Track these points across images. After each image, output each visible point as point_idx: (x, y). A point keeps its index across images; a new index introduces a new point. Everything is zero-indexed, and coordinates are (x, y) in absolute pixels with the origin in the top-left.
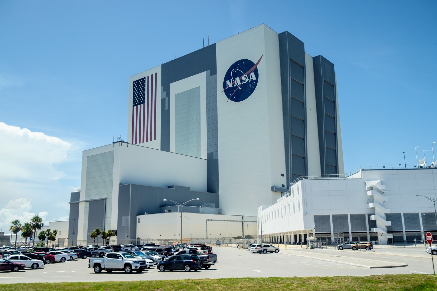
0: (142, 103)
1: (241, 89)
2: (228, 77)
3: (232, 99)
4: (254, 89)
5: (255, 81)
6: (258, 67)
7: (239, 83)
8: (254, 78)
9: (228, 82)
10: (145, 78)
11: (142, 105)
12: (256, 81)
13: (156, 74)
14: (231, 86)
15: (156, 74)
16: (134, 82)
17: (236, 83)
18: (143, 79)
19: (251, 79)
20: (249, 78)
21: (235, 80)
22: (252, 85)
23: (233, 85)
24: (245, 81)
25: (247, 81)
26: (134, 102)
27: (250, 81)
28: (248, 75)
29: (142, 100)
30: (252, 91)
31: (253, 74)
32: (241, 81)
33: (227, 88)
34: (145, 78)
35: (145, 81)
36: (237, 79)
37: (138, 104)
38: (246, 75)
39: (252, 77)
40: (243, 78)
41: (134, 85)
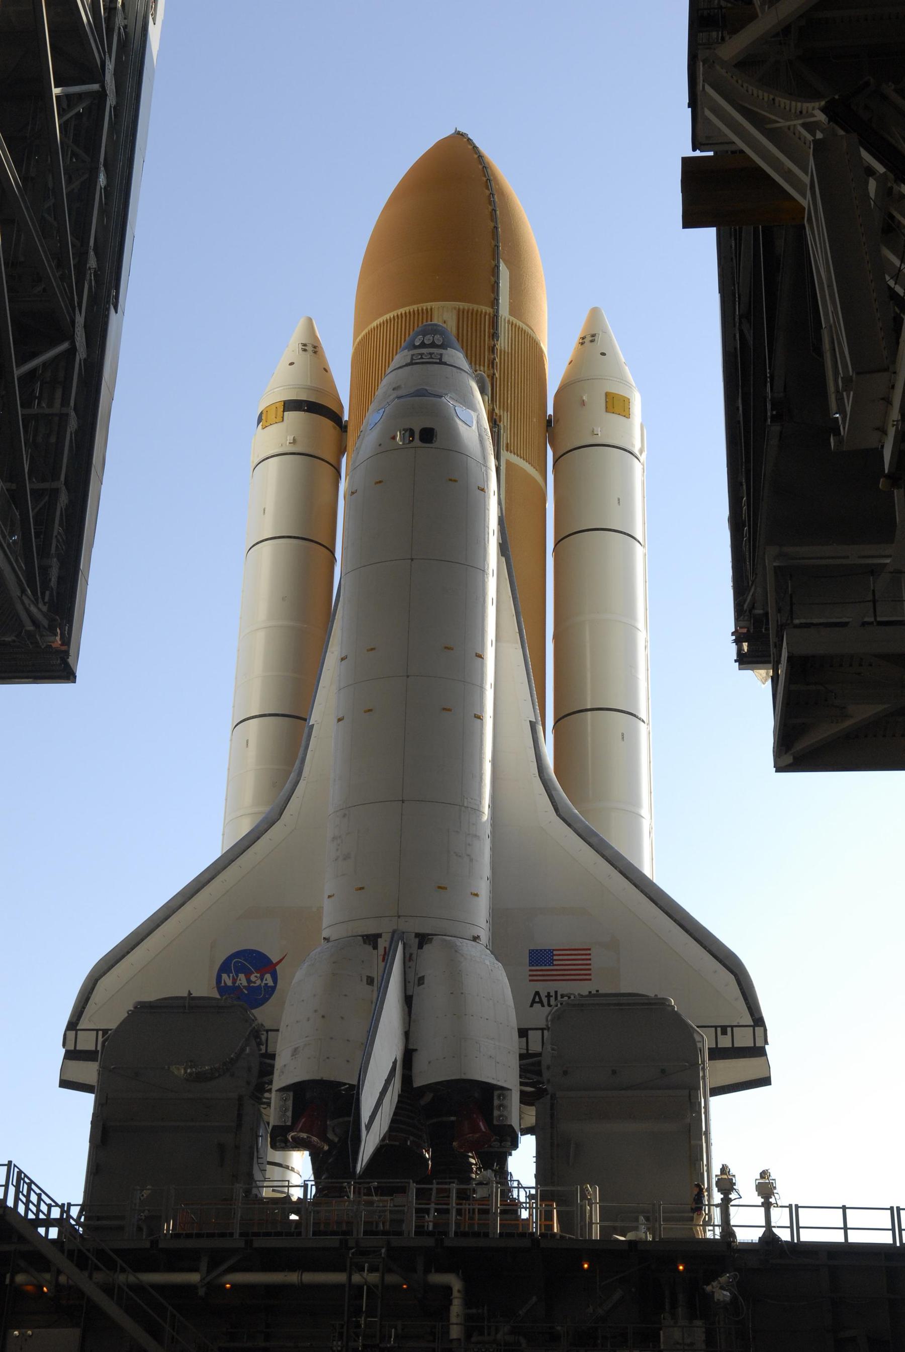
2: (225, 967)
4: (268, 999)
5: (270, 987)
6: (277, 968)
7: (245, 983)
8: (271, 983)
9: (224, 976)
12: (273, 989)
14: (229, 983)
17: (238, 982)
19: (264, 982)
20: (262, 980)
24: (255, 983)
25: (258, 982)
30: (265, 1000)
31: (268, 976)
32: (249, 981)
33: (223, 984)
36: (242, 976)
40: (253, 978)
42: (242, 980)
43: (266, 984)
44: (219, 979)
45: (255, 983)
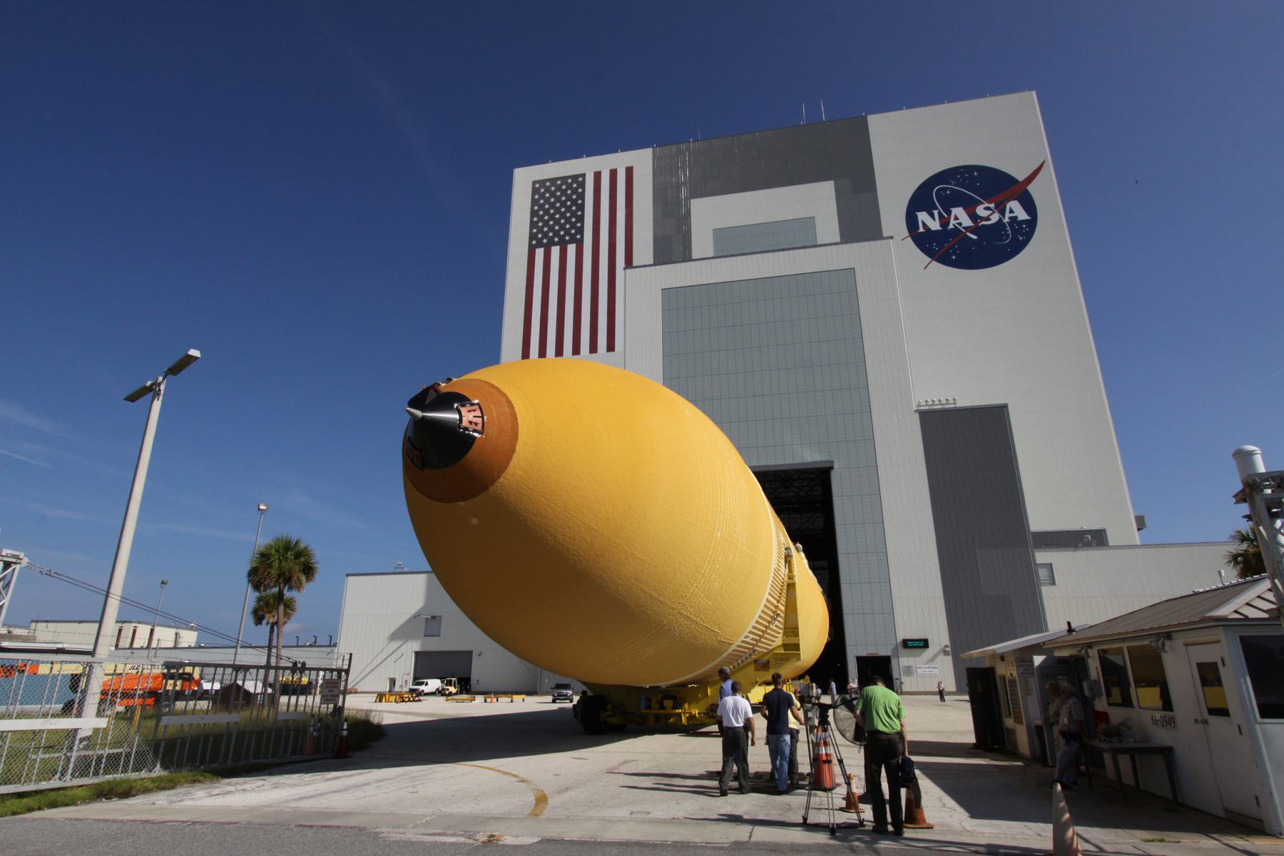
0: (570, 242)
1: (975, 237)
2: (920, 200)
3: (944, 260)
6: (1030, 188)
7: (966, 222)
8: (1022, 215)
10: (583, 176)
11: (572, 249)
12: (1032, 224)
13: (629, 171)
14: (935, 225)
15: (629, 171)
16: (534, 183)
18: (575, 178)
19: (1008, 215)
20: (1002, 213)
21: (949, 213)
22: (1015, 232)
23: (944, 222)
25: (995, 218)
26: (532, 237)
27: (1006, 220)
28: (996, 207)
29: (567, 232)
32: (974, 217)
33: (921, 230)
34: (583, 176)
35: (582, 185)
37: (551, 243)
38: (992, 206)
39: (1011, 211)
40: (980, 211)
41: (535, 191)
42: (960, 216)
43: (1014, 219)
44: (911, 222)
45: (988, 219)
